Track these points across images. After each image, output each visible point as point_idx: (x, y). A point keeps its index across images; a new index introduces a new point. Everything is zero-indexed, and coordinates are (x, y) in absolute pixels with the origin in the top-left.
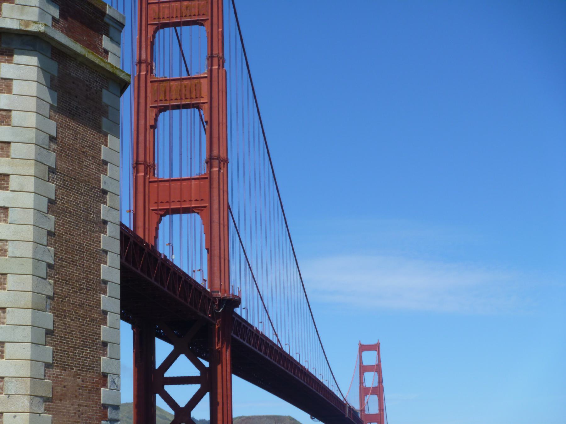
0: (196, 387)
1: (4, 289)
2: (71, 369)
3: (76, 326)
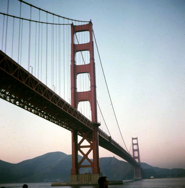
0: (89, 149)
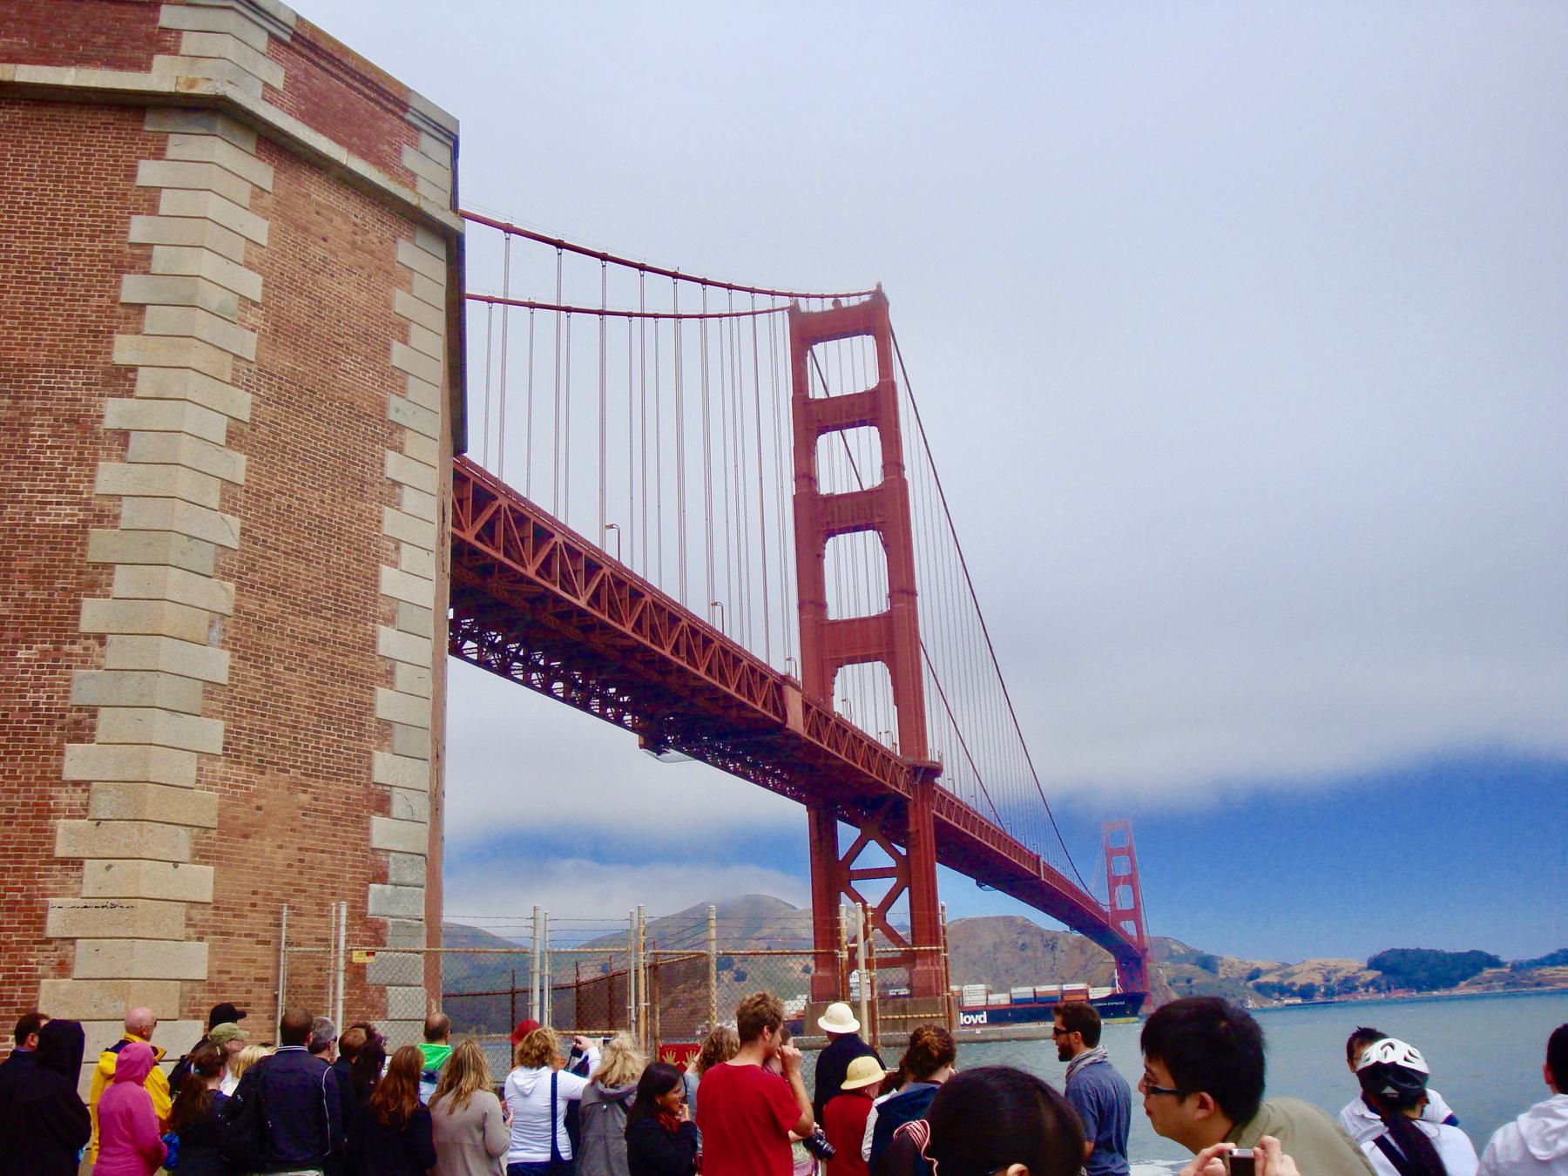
0: (890, 882)
1: (106, 596)
2: (279, 770)
3: (301, 683)
